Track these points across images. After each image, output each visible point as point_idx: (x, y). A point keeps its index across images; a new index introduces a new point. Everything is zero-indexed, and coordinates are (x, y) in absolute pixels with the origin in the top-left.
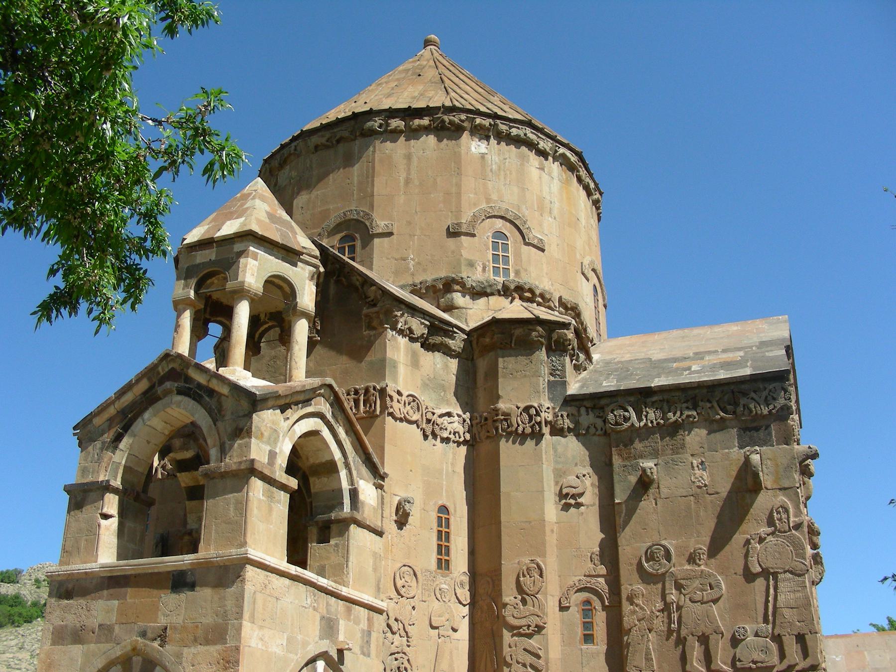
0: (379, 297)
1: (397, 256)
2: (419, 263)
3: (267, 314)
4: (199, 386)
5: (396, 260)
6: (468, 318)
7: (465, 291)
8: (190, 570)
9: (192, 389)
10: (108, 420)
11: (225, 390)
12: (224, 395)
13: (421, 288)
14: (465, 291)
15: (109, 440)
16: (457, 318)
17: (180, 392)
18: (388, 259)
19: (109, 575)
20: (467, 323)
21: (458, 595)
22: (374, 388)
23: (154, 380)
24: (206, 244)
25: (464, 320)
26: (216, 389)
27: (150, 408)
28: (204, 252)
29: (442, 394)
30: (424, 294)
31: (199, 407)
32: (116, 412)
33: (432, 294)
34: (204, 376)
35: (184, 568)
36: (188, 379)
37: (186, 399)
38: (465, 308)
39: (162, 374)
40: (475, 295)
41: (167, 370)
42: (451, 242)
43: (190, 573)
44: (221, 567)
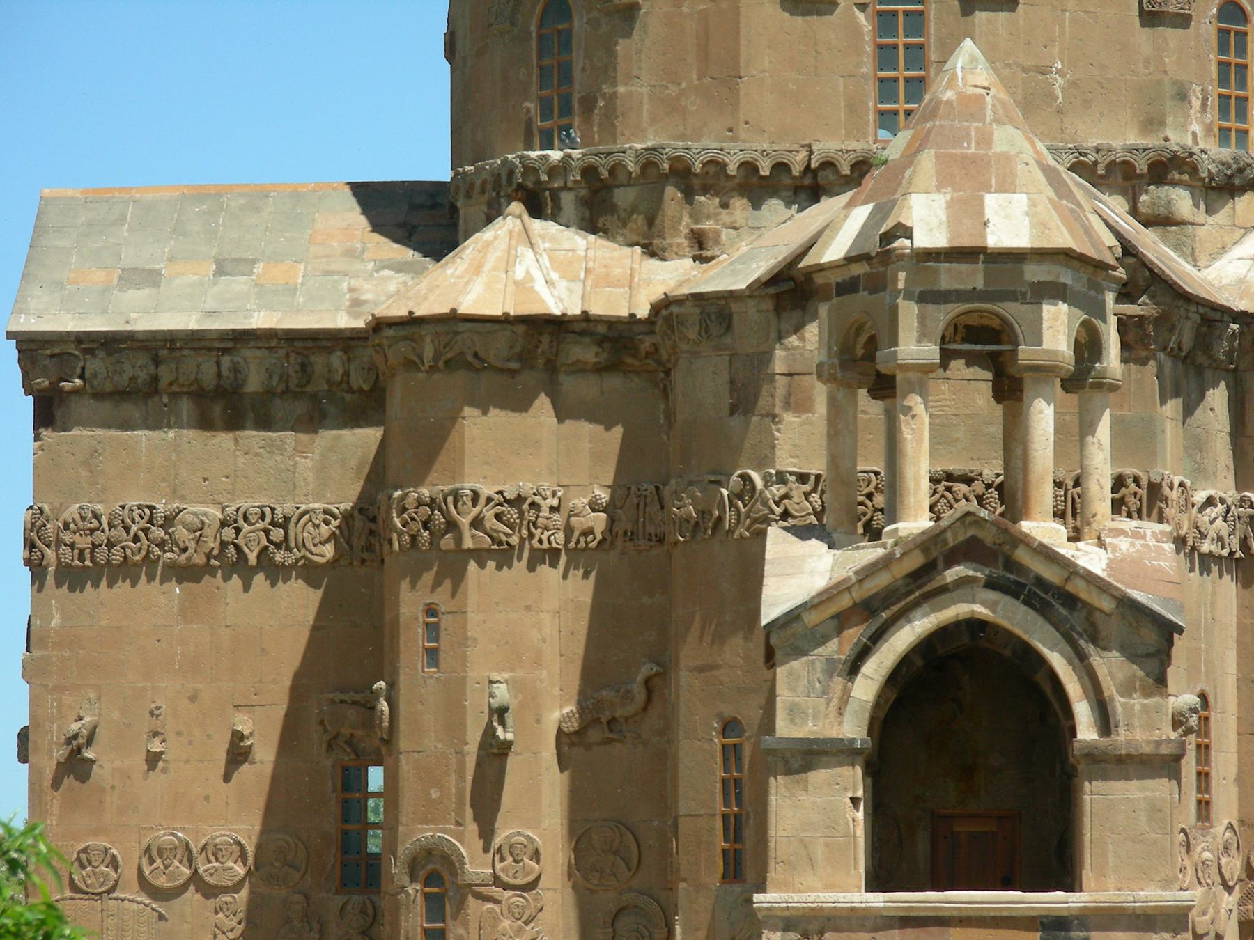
0: (1142, 283)
1: (1029, 63)
2: (1074, 84)
3: (960, 328)
4: (1040, 582)
5: (1025, 70)
6: (1197, 245)
7: (1195, 183)
8: (1077, 917)
9: (1023, 586)
10: (833, 617)
11: (1106, 604)
12: (1101, 611)
13: (1096, 163)
14: (1195, 183)
15: (843, 657)
16: (1177, 247)
17: (991, 585)
18: (1008, 66)
19: (902, 914)
20: (1195, 260)
21: (1223, 870)
22: (1136, 480)
23: (934, 554)
24: (966, 253)
25: (1188, 251)
26: (1083, 595)
27: (925, 605)
28: (955, 265)
29: (1198, 457)
30: (1101, 176)
31: (1040, 620)
32: (851, 604)
33: (1120, 180)
34: (1057, 569)
35: (1065, 914)
36: (1011, 564)
37: (1007, 600)
38: (1193, 224)
39: (951, 544)
40: (1213, 195)
41: (961, 538)
42: (1144, 38)
43: (1076, 922)
44: (1138, 916)
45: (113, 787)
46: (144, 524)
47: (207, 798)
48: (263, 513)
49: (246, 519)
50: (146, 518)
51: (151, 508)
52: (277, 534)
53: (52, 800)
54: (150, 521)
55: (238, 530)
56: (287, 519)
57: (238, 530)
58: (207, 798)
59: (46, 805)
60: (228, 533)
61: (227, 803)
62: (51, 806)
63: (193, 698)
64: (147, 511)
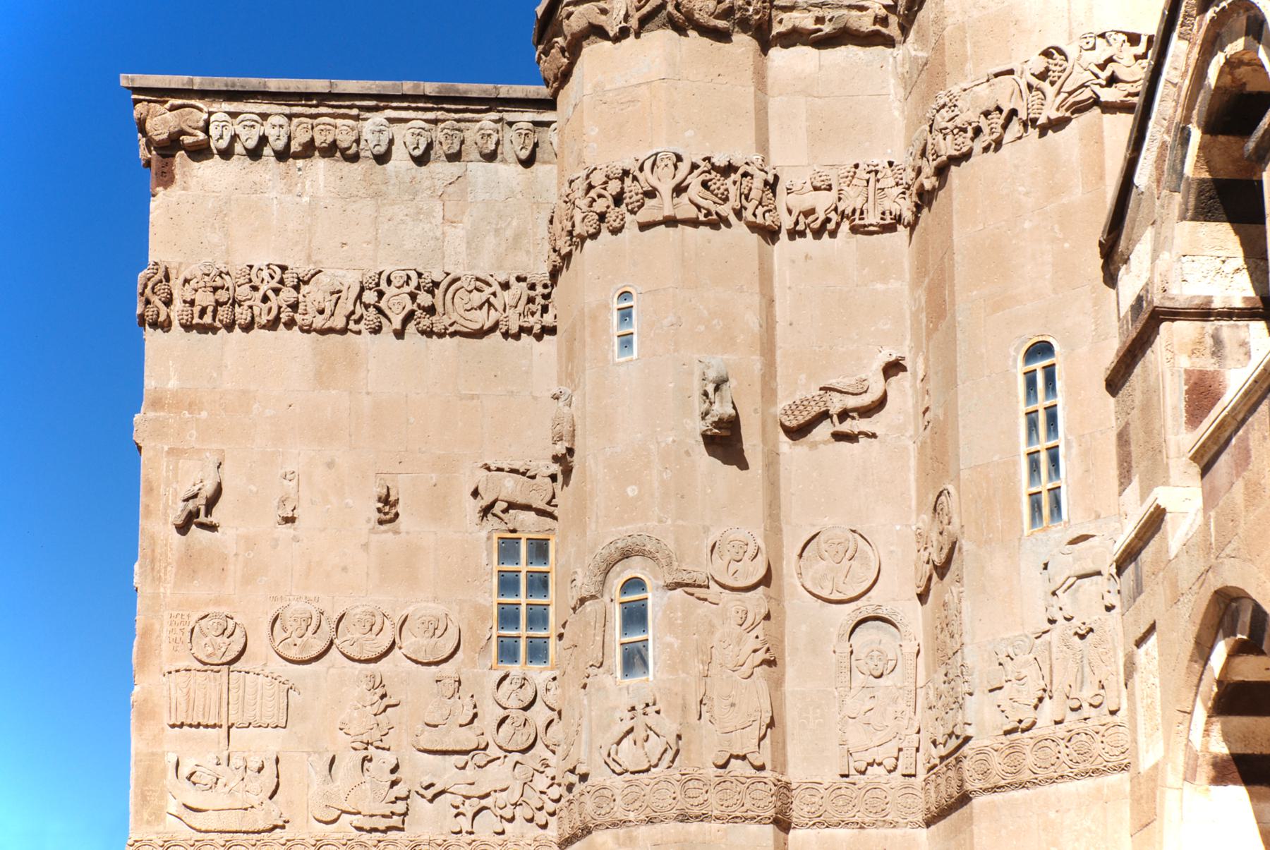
45: (236, 555)
46: (274, 284)
47: (345, 569)
48: (409, 278)
49: (389, 282)
50: (277, 278)
51: (284, 268)
52: (425, 300)
53: (165, 568)
54: (281, 282)
55: (381, 294)
56: (436, 284)
57: (381, 294)
58: (345, 569)
59: (159, 572)
60: (369, 297)
61: (368, 574)
62: (165, 574)
63: (330, 465)
64: (278, 271)
